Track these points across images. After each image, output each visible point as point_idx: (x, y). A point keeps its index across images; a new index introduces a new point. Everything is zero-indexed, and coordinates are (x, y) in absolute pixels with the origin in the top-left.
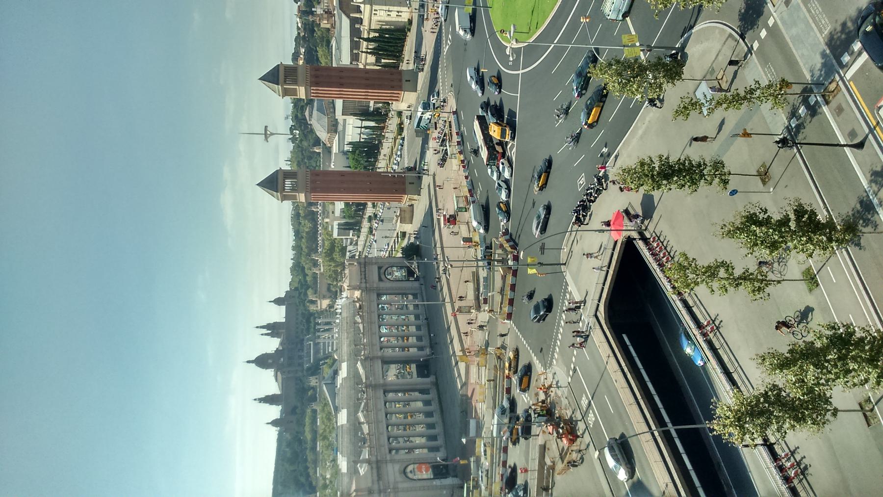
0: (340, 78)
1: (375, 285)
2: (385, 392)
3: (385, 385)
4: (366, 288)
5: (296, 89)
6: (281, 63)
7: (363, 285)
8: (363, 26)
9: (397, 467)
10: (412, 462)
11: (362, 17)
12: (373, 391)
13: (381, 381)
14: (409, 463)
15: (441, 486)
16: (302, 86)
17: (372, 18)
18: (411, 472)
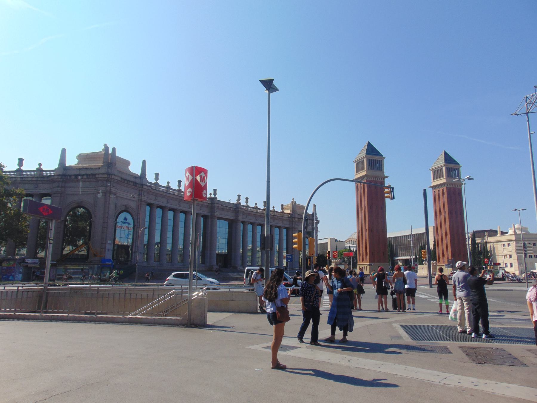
0: (455, 212)
1: (296, 226)
2: (205, 217)
3: (213, 217)
4: (295, 218)
5: (443, 176)
6: (461, 166)
7: (296, 216)
8: (488, 238)
9: (133, 205)
10: (136, 223)
11: (498, 235)
12: (207, 204)
13: (217, 214)
14: (136, 221)
15: (105, 248)
16: (446, 180)
17: (498, 243)
18: (126, 219)
